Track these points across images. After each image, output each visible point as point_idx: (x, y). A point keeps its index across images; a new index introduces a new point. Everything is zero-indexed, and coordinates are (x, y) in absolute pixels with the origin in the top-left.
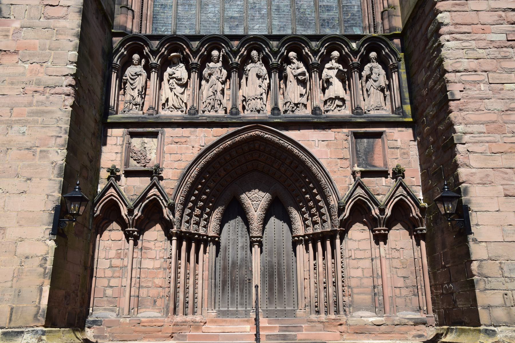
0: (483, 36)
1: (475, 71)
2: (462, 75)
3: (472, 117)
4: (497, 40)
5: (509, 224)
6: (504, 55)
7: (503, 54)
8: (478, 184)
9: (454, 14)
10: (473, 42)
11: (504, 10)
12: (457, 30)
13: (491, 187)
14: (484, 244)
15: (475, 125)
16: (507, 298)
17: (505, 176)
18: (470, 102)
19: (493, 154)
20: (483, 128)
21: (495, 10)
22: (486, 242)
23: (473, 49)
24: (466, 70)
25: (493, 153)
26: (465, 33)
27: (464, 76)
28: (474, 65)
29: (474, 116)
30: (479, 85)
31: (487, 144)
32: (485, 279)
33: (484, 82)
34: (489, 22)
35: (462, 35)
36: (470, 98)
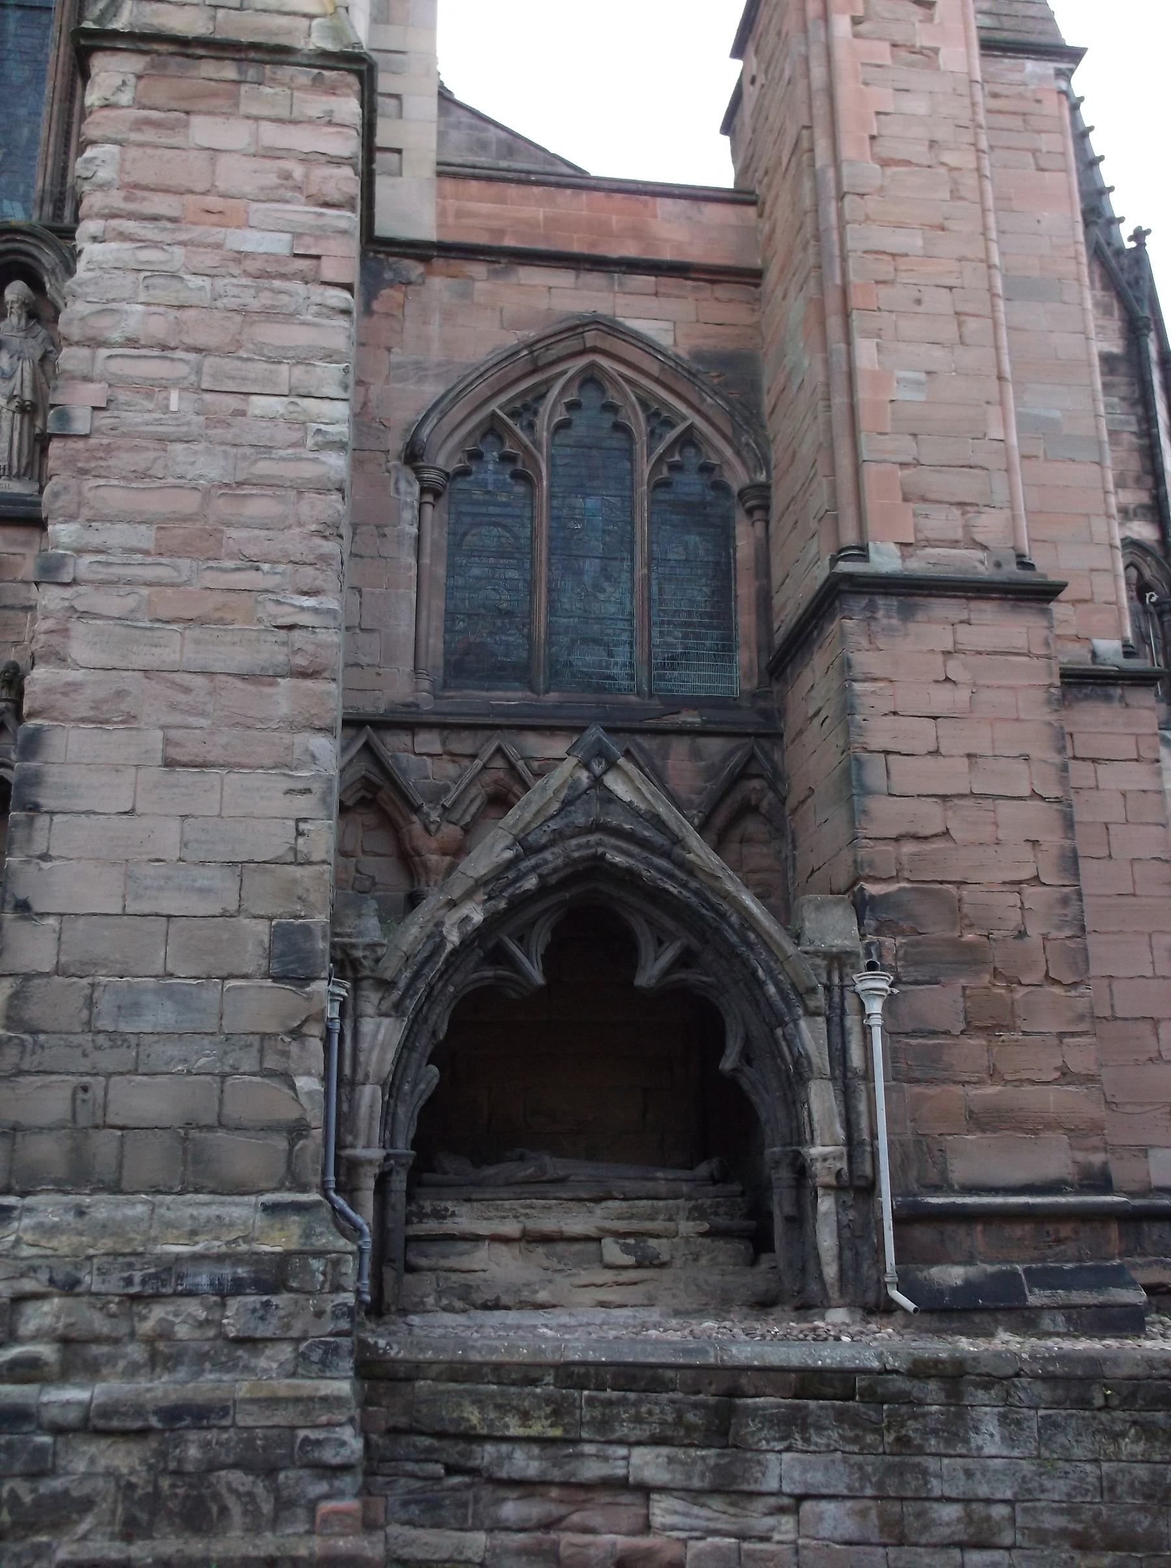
0: (217, 234)
1: (164, 348)
2: (110, 357)
3: (115, 497)
4: (261, 250)
5: (154, 857)
6: (269, 302)
7: (266, 299)
8: (83, 720)
9: (133, 153)
10: (179, 251)
11: (303, 157)
12: (131, 207)
13: (125, 733)
14: (51, 921)
15: (119, 526)
16: (84, 1101)
17: (181, 698)
18: (119, 448)
19: (157, 625)
20: (144, 536)
21: (272, 154)
22: (62, 915)
23: (174, 276)
24: (132, 342)
25: (158, 620)
26: (155, 218)
27: (119, 360)
28: (158, 327)
29: (120, 493)
30: (164, 394)
31: (145, 591)
32: (25, 1037)
33: (186, 384)
34: (247, 189)
35: (146, 224)
36: (124, 435)
